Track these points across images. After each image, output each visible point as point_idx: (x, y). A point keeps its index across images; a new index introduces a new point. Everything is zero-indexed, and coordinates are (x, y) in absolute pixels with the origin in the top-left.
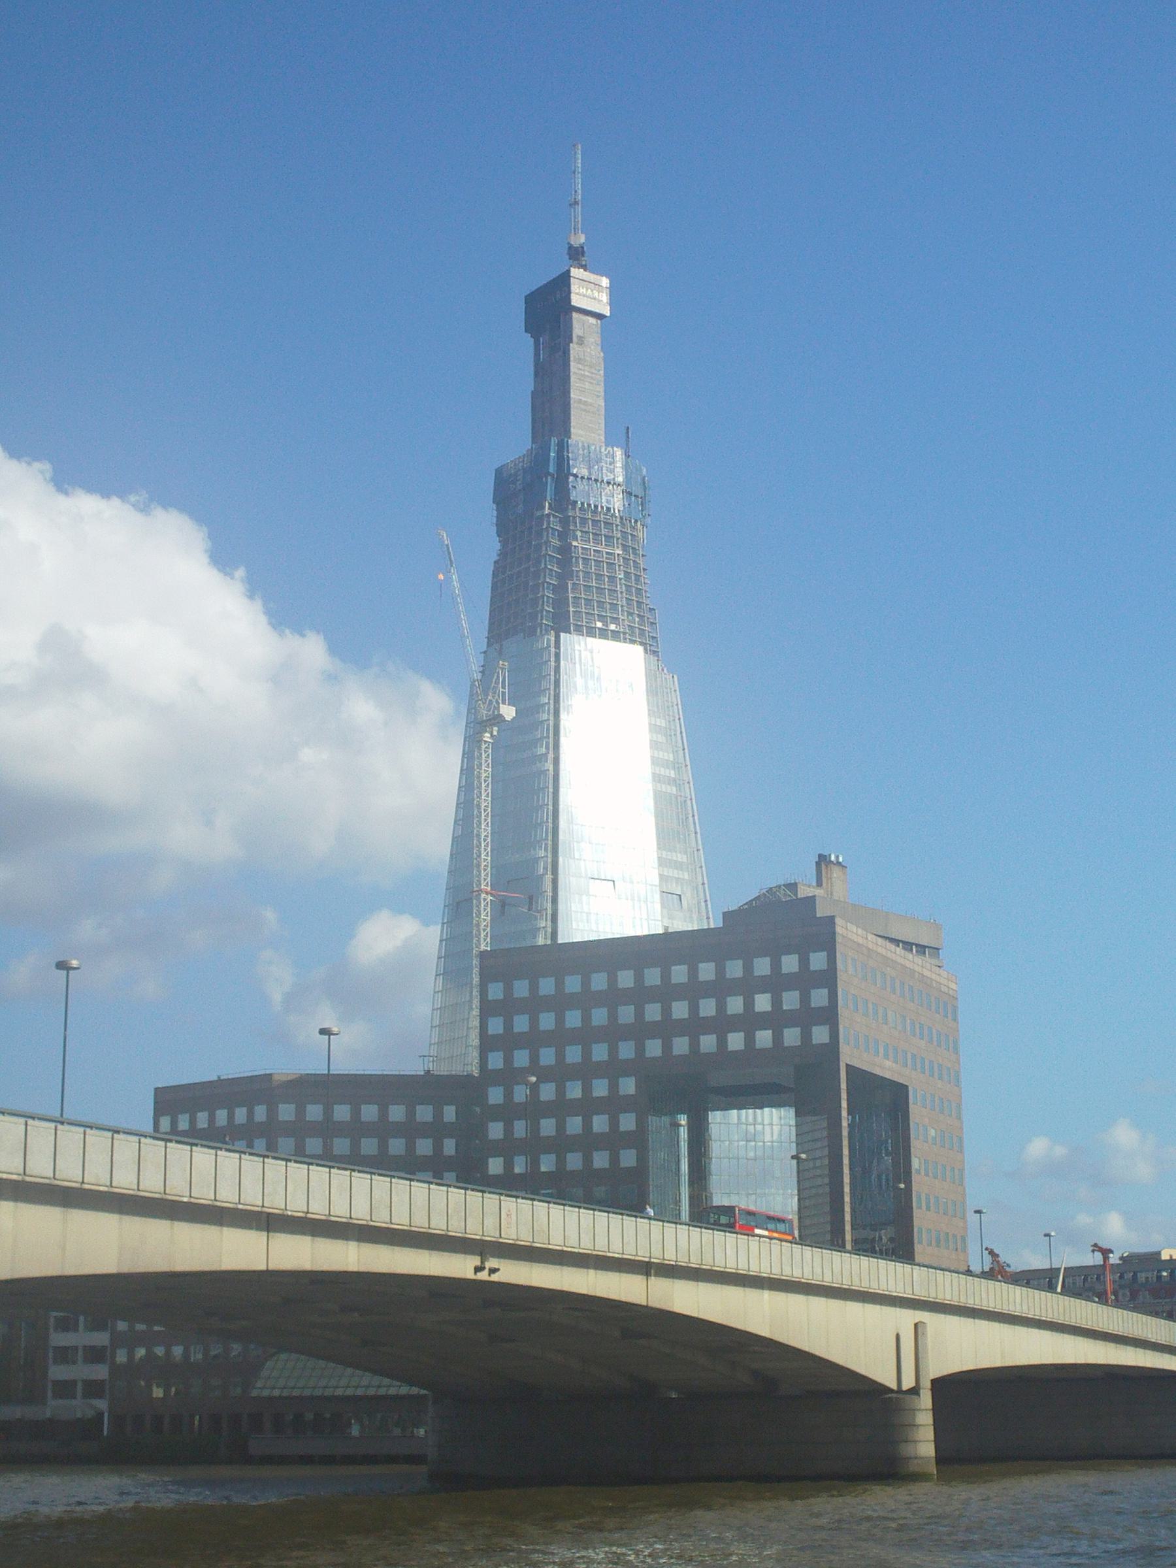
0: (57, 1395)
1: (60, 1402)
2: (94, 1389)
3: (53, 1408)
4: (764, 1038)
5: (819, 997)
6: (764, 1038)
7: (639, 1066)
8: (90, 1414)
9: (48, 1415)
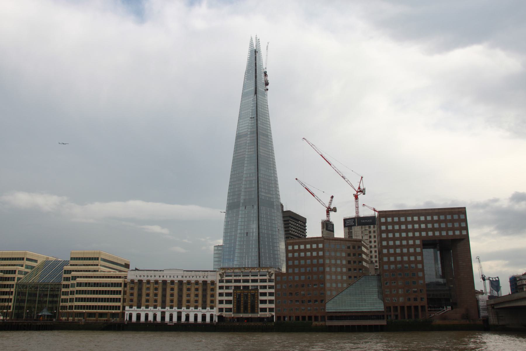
0: (261, 312)
1: (263, 313)
2: (271, 310)
3: (260, 314)
4: (451, 233)
5: (463, 225)
8: (270, 316)
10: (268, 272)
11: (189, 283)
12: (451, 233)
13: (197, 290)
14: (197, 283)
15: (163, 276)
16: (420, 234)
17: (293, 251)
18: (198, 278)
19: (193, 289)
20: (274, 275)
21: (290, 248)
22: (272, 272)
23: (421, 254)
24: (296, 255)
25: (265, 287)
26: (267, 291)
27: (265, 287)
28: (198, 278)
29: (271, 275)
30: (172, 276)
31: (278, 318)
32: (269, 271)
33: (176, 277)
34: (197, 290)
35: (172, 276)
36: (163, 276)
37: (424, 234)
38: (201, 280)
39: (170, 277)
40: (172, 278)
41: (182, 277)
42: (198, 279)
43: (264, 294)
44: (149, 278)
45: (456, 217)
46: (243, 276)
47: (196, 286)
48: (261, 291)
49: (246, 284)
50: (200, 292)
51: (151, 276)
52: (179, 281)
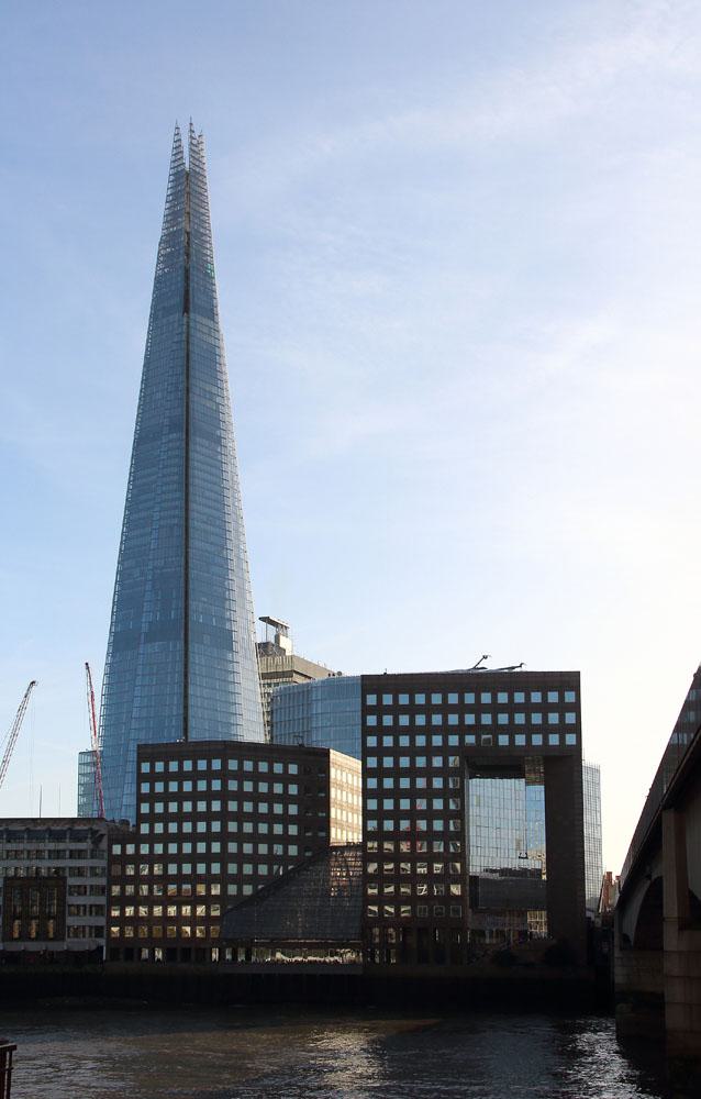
3: (70, 943)
4: (537, 740)
5: (570, 718)
6: (520, 740)
7: (461, 750)
8: (94, 947)
9: (65, 948)
10: (91, 829)
12: (537, 740)
16: (462, 740)
17: (152, 778)
20: (105, 840)
21: (146, 768)
22: (103, 832)
23: (460, 794)
24: (159, 787)
25: (80, 872)
26: (89, 881)
27: (80, 872)
29: (97, 839)
31: (113, 953)
32: (95, 827)
37: (470, 739)
43: (81, 890)
45: (553, 697)
46: (30, 839)
48: (71, 881)
49: (35, 863)
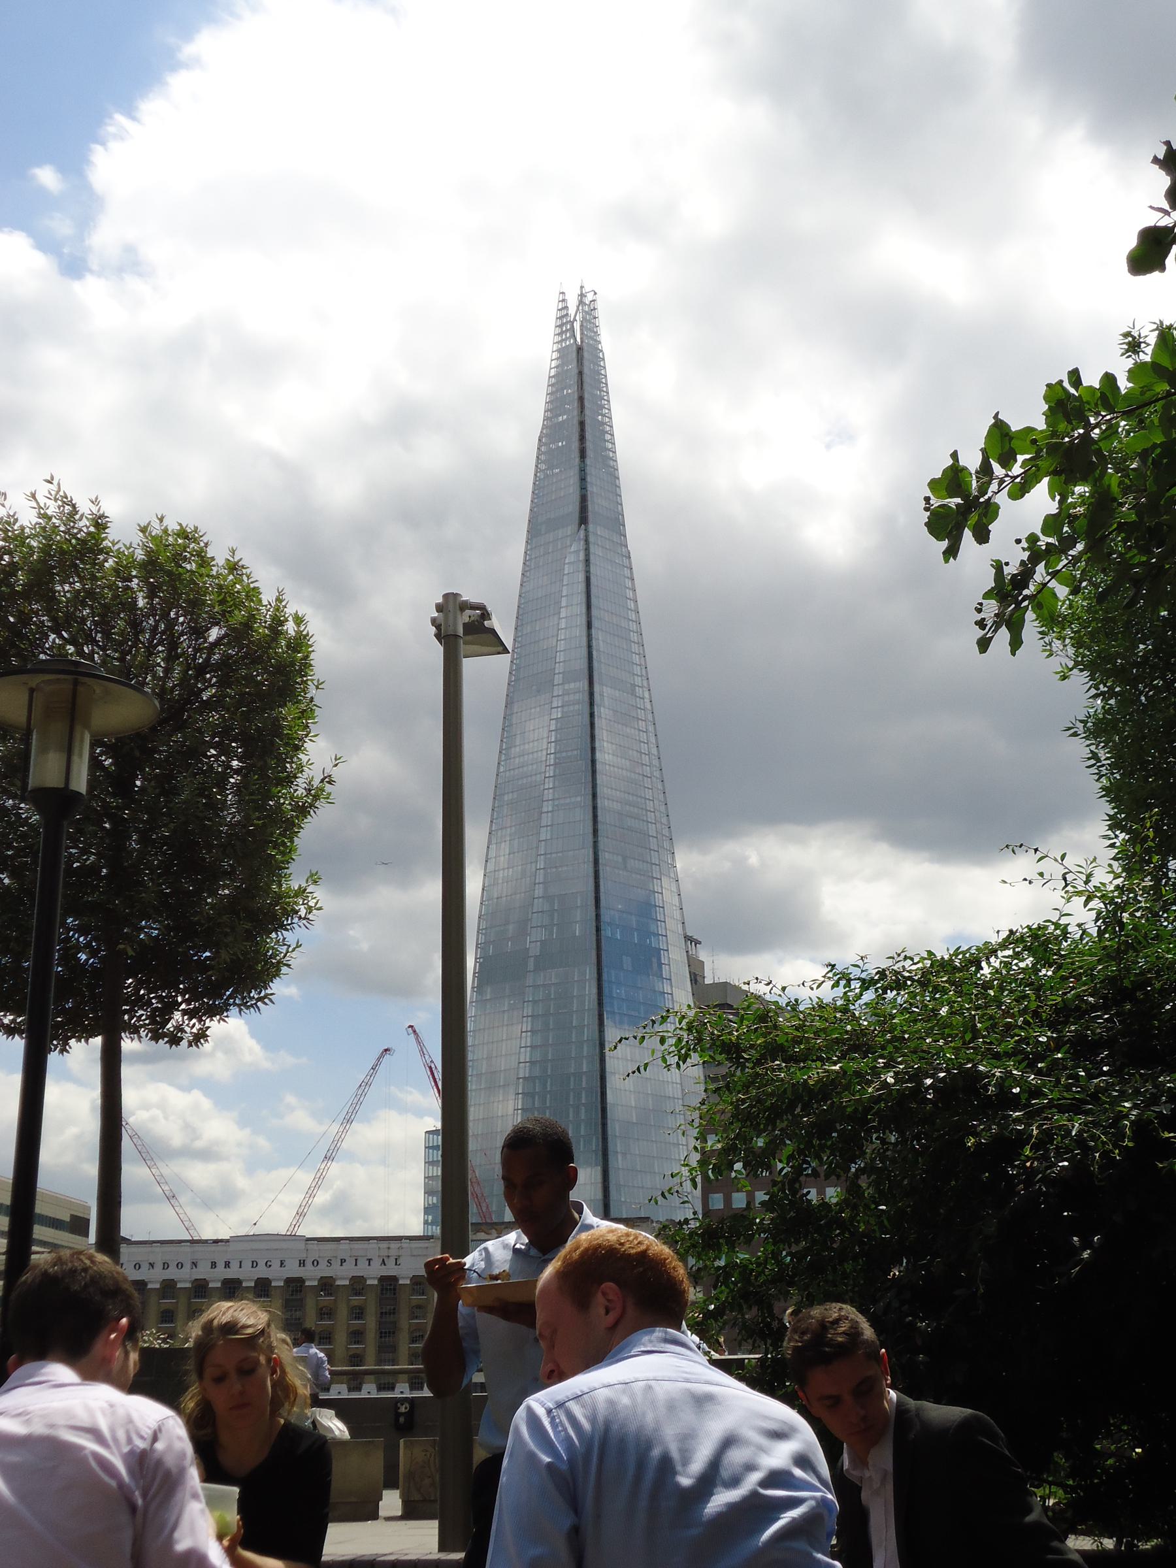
11: (327, 1285)
13: (358, 1313)
14: (358, 1285)
15: (227, 1264)
18: (363, 1263)
19: (343, 1312)
28: (363, 1263)
30: (262, 1263)
33: (276, 1264)
34: (358, 1313)
35: (262, 1263)
36: (227, 1264)
38: (373, 1273)
39: (254, 1264)
40: (262, 1272)
41: (302, 1263)
42: (362, 1270)
44: (172, 1273)
47: (356, 1300)
50: (371, 1323)
51: (180, 1265)
52: (289, 1281)
